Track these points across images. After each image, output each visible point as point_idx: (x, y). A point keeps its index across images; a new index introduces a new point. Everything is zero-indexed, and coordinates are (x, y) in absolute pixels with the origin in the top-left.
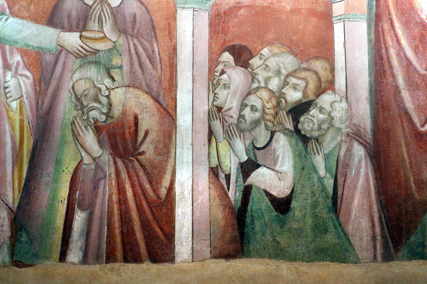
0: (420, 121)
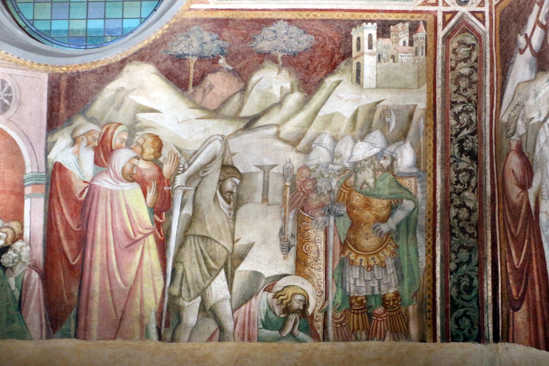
0: (72, 258)
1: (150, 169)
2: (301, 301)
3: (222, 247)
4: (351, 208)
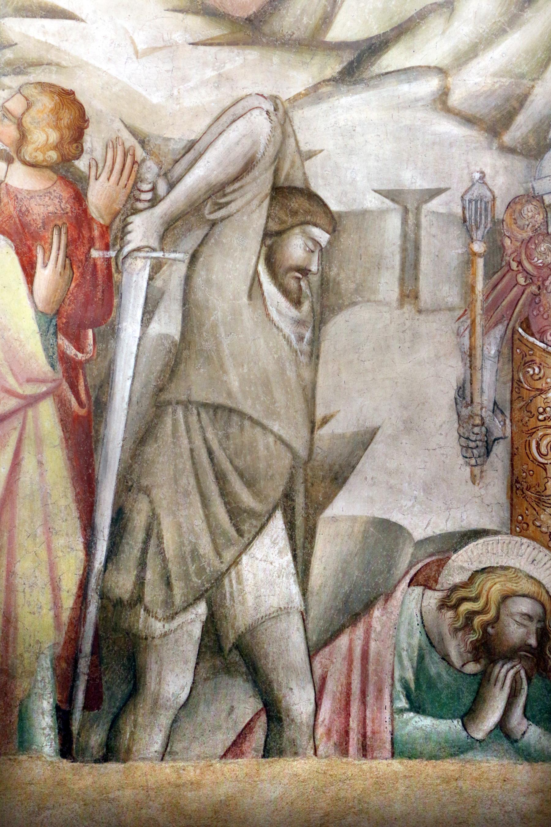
1: (47, 192)
2: (530, 618)
3: (275, 441)
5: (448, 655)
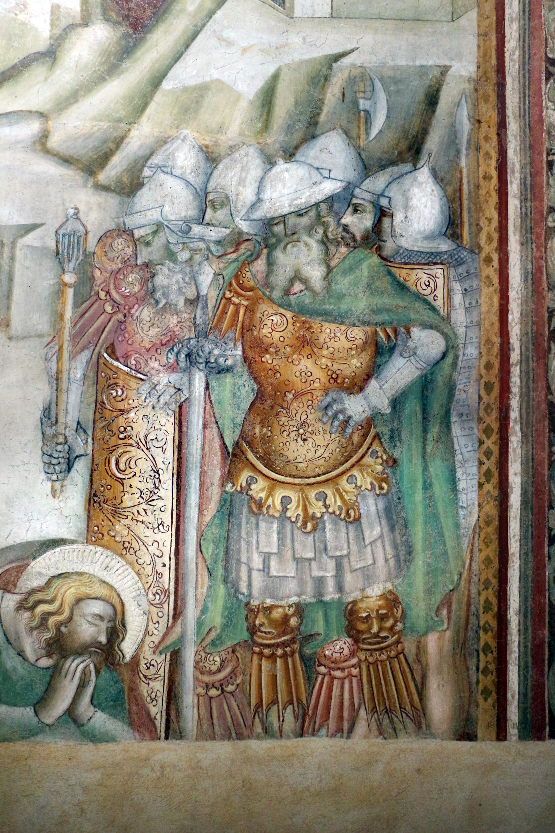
2: (101, 618)
4: (255, 349)
5: (24, 651)
